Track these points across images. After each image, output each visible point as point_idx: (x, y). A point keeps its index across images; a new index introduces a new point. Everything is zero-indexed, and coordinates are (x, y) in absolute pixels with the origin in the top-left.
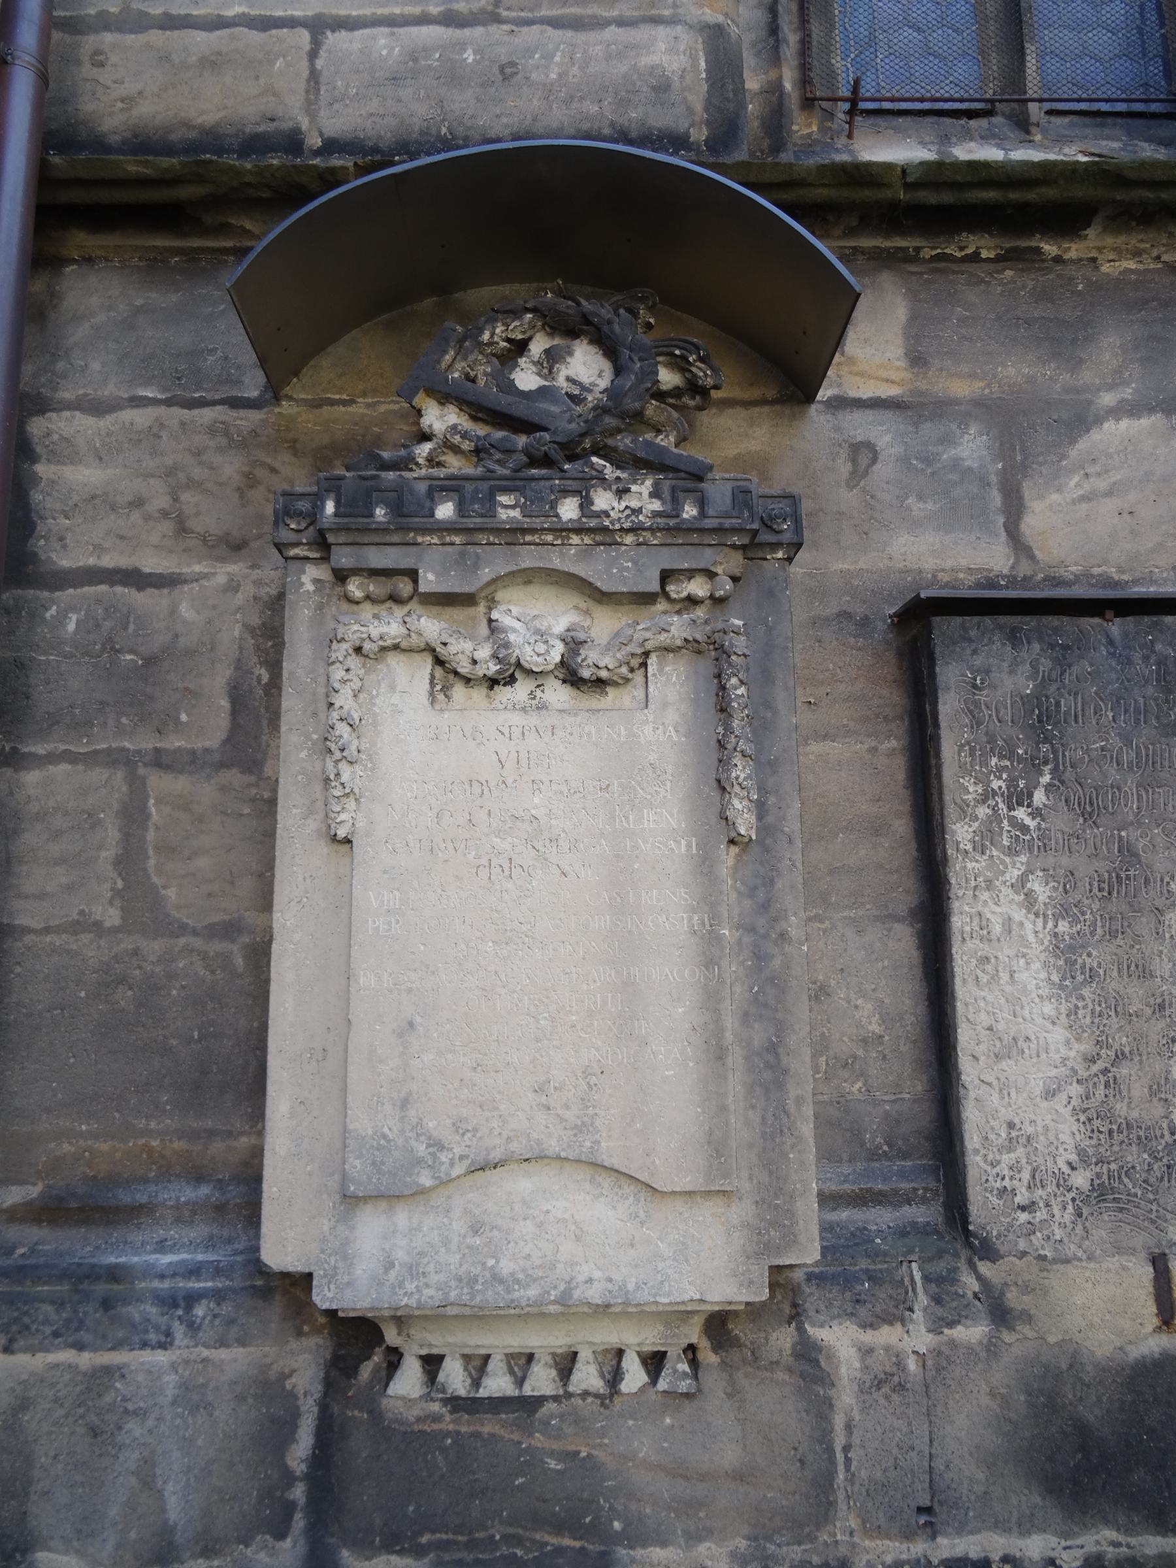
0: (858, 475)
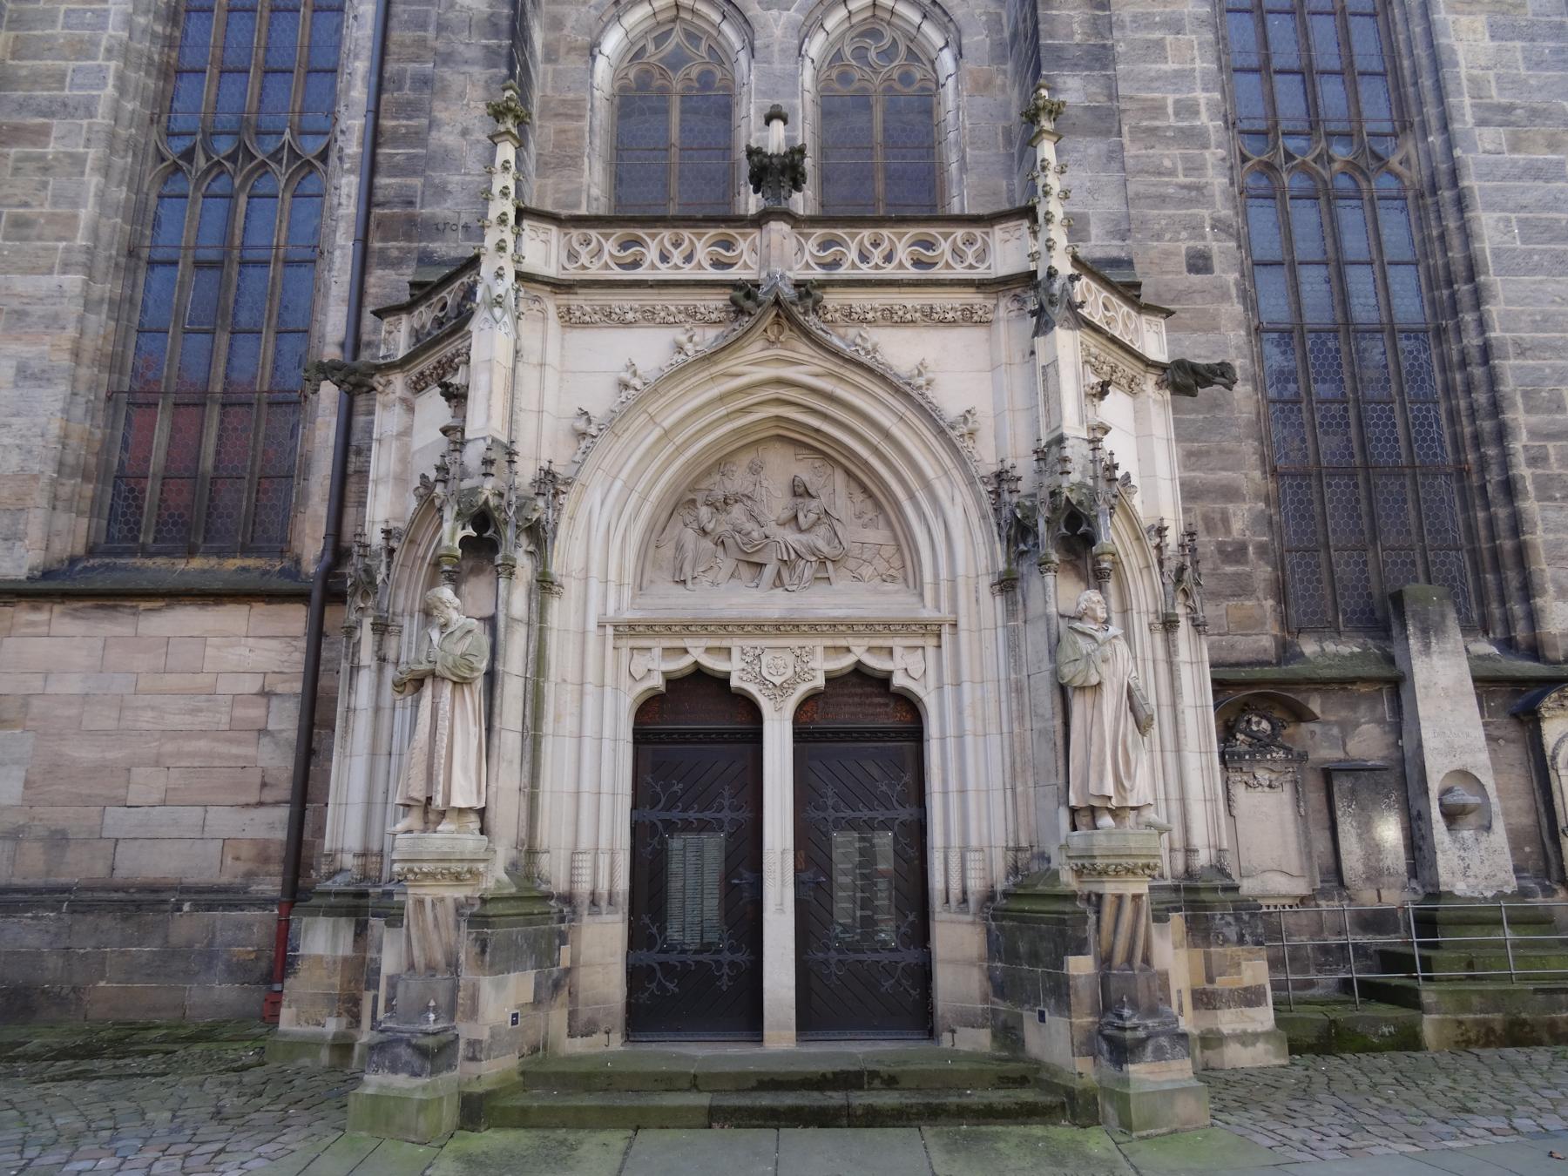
0: (1312, 738)
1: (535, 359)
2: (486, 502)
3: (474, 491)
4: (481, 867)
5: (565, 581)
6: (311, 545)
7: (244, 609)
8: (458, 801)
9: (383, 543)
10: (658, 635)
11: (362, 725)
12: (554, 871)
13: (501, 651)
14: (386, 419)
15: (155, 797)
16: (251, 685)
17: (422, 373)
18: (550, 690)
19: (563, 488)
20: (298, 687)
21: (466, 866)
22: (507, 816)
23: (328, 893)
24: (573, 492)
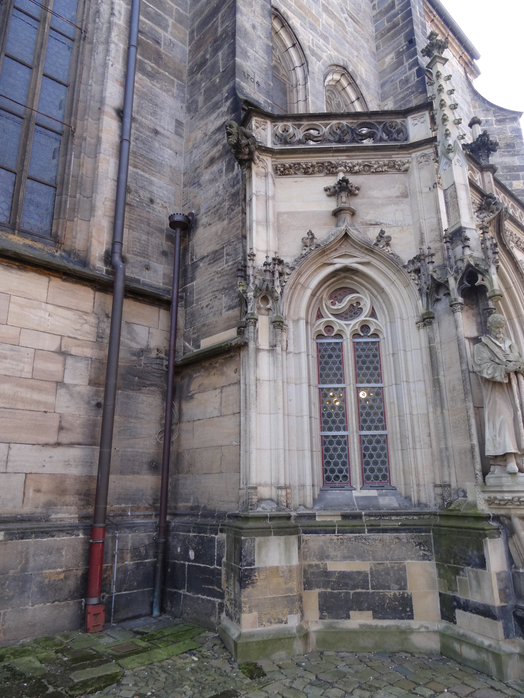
7: (44, 280)
16: (52, 344)
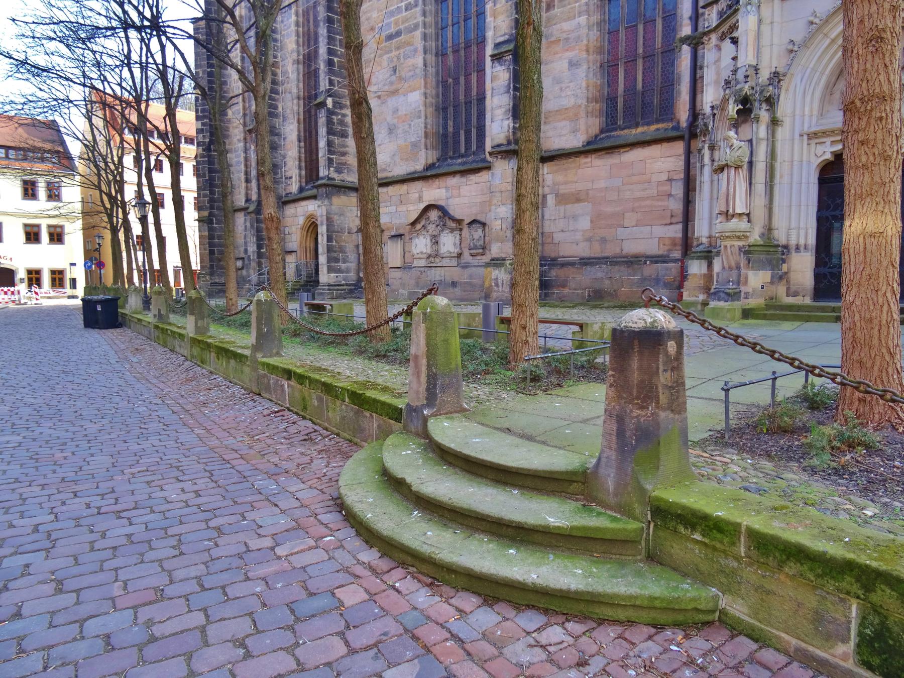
1: (768, 21)
2: (746, 93)
3: (741, 90)
4: (748, 234)
5: (784, 119)
6: (683, 115)
8: (738, 211)
9: (711, 112)
10: (829, 136)
11: (706, 187)
12: (780, 236)
13: (754, 153)
14: (708, 55)
15: (634, 223)
16: (664, 177)
17: (723, 32)
18: (777, 165)
19: (782, 78)
20: (682, 176)
21: (742, 234)
22: (759, 215)
23: (697, 252)
24: (787, 79)
